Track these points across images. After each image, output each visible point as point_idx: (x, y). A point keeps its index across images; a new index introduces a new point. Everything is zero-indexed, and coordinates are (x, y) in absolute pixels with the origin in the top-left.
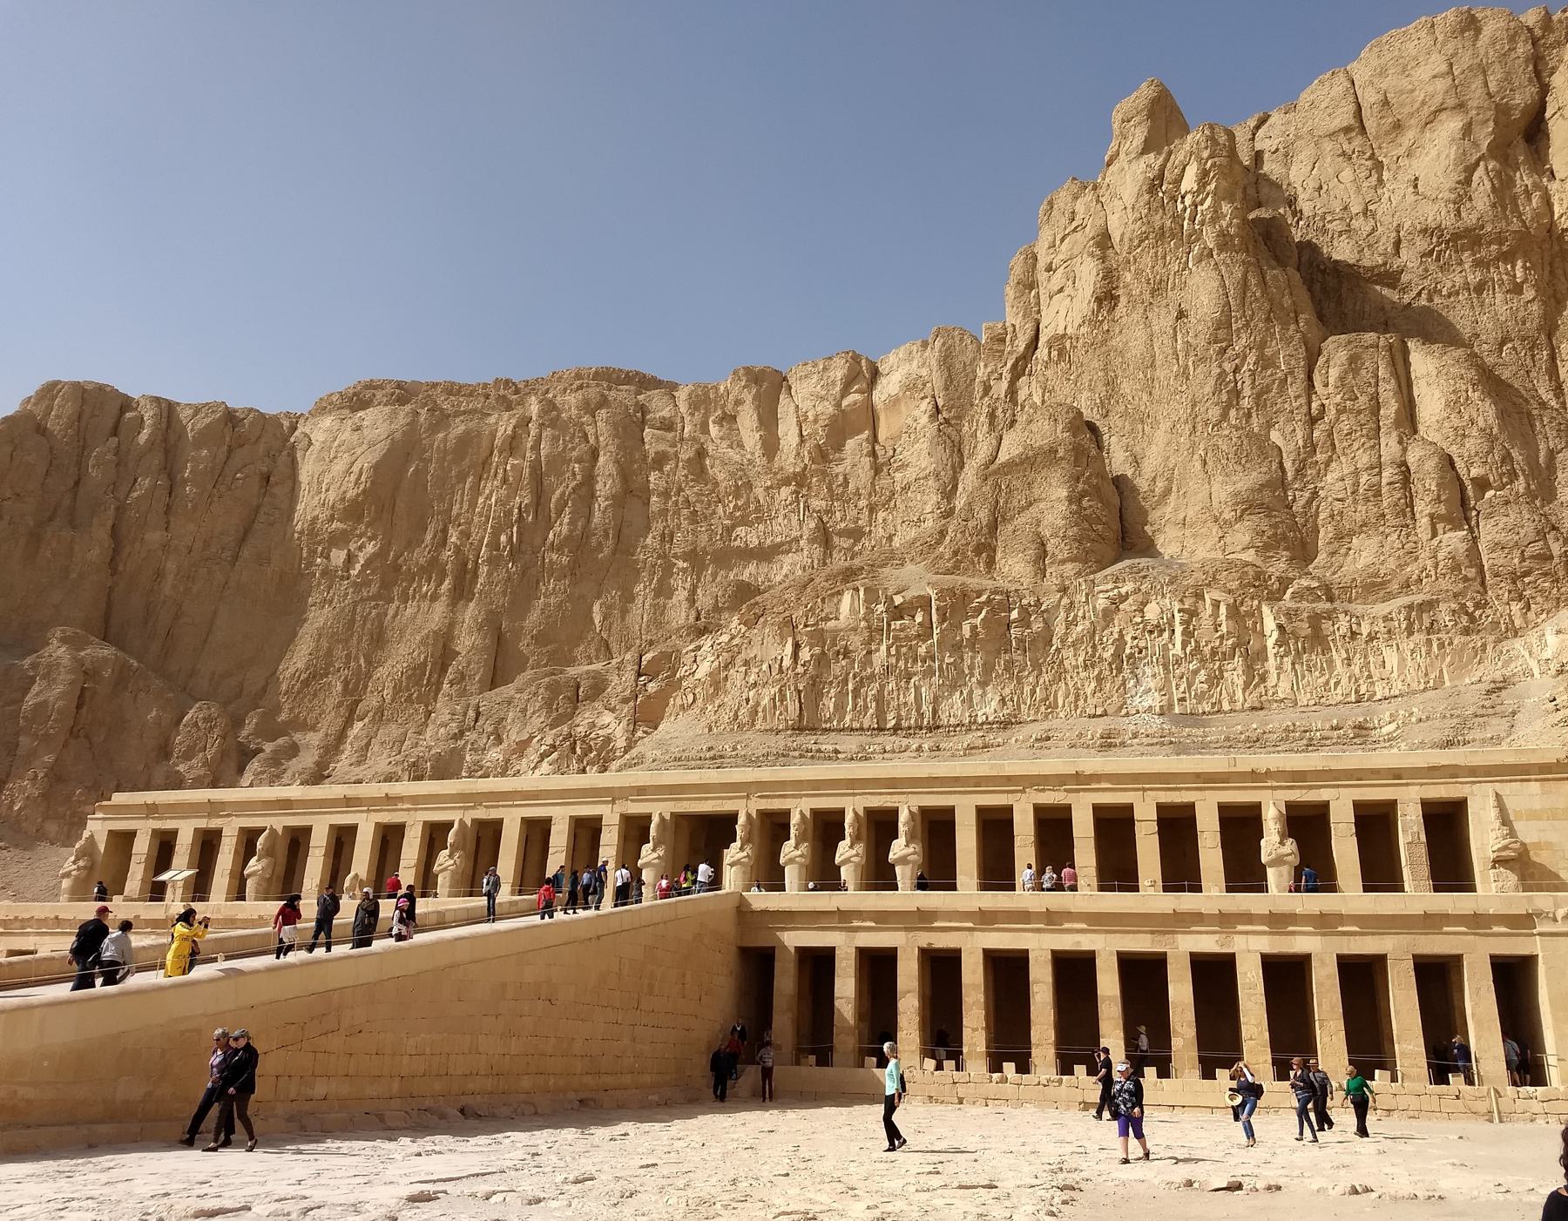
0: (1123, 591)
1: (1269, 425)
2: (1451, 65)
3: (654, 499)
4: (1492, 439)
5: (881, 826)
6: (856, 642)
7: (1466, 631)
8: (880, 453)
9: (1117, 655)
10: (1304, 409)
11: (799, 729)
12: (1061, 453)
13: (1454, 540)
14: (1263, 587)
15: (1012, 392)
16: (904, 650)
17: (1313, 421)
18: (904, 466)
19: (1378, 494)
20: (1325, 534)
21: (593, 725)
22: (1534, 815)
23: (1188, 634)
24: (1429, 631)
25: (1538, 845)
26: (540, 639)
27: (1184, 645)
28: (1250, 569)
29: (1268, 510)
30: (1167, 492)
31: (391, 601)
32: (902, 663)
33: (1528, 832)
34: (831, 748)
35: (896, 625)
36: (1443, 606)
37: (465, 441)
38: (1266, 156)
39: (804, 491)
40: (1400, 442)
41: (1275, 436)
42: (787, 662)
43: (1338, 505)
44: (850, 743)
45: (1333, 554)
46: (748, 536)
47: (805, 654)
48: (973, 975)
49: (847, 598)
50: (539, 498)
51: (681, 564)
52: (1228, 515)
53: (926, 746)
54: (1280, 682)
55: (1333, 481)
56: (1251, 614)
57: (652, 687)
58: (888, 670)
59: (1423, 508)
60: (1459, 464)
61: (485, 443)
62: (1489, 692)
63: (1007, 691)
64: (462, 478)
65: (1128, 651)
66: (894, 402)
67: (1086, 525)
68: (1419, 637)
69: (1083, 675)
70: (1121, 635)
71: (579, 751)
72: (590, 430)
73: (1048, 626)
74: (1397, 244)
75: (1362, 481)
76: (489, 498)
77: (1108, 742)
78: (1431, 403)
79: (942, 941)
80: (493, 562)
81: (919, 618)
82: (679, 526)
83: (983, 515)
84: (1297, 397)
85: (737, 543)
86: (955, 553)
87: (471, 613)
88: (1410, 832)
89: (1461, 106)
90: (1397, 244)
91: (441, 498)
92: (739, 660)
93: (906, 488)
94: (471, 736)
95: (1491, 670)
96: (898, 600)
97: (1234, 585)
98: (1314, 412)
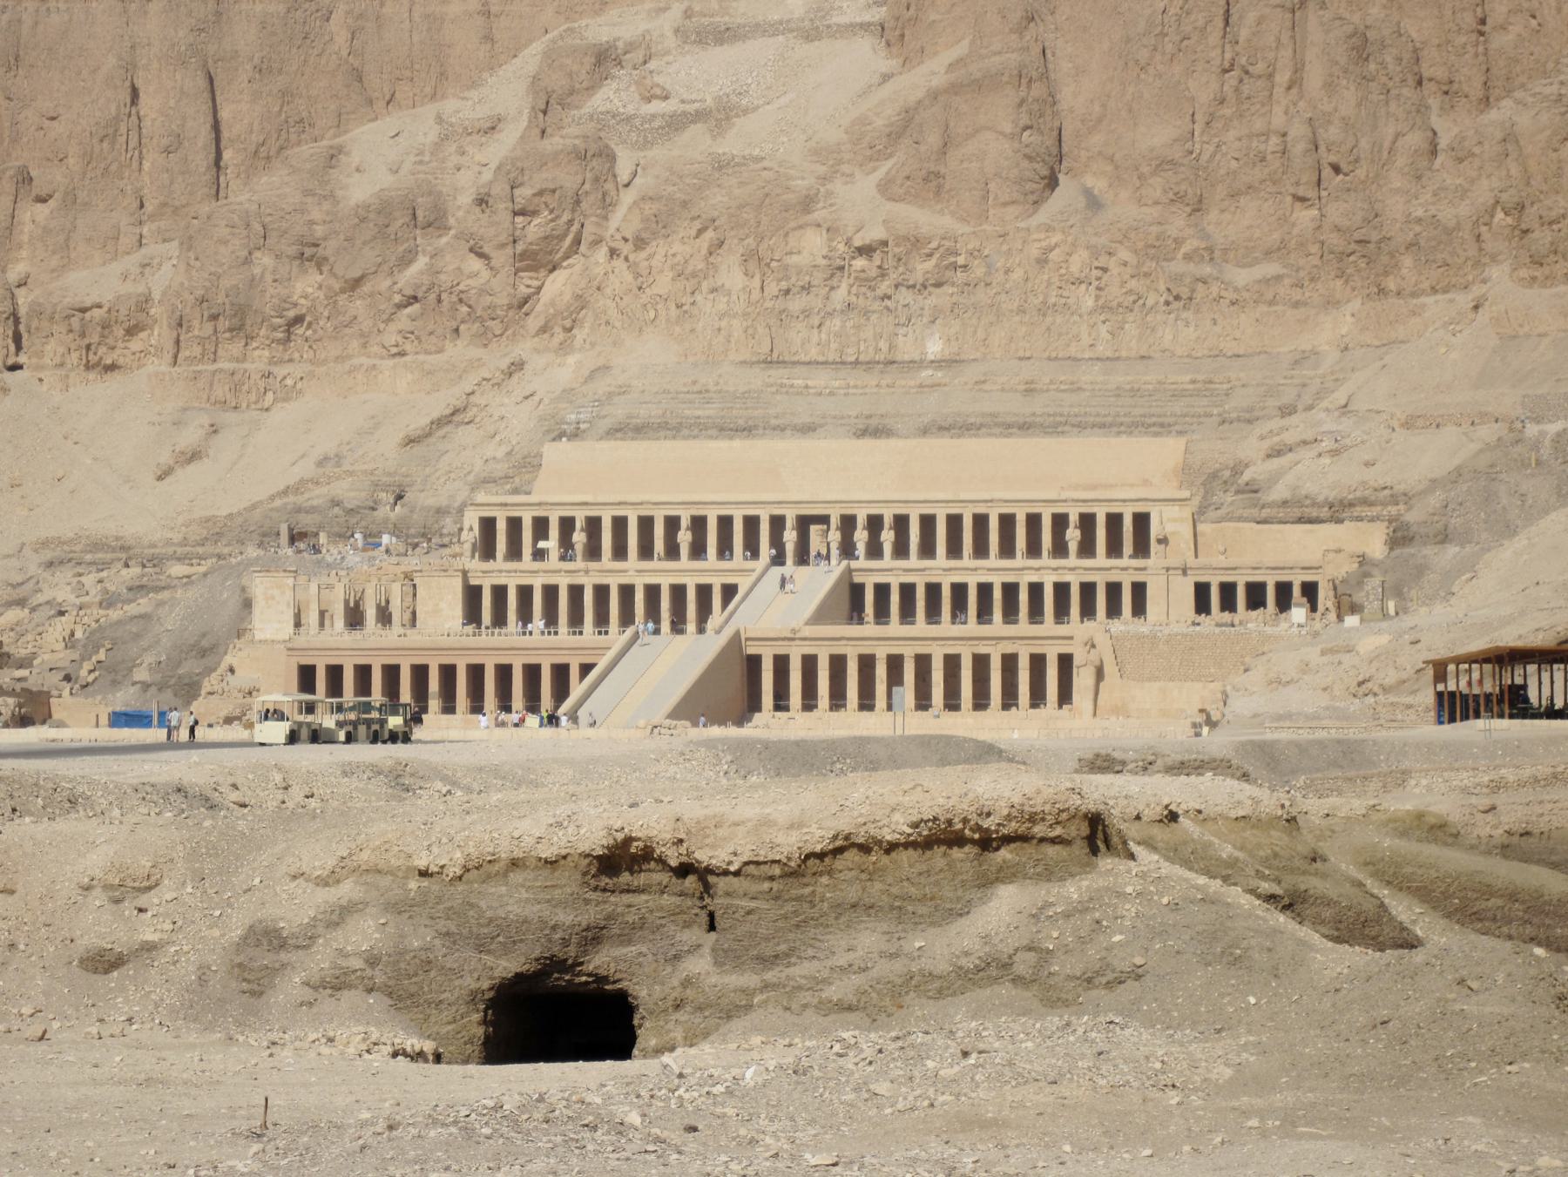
0: (1054, 241)
5: (901, 522)
7: (1296, 305)
9: (1044, 303)
10: (1218, 62)
11: (768, 363)
12: (1005, 79)
13: (1305, 217)
16: (863, 289)
17: (1226, 71)
19: (1263, 159)
20: (1221, 191)
22: (1175, 520)
23: (1099, 288)
24: (1271, 303)
25: (1173, 533)
27: (1097, 298)
28: (1155, 229)
30: (1100, 120)
32: (861, 301)
33: (1169, 528)
34: (800, 382)
35: (860, 263)
36: (1287, 281)
40: (1286, 113)
41: (1191, 83)
42: (756, 295)
43: (1234, 164)
44: (820, 379)
45: (1223, 211)
48: (946, 593)
53: (884, 383)
56: (1147, 275)
57: (534, 229)
60: (1322, 149)
62: (1296, 362)
63: (953, 331)
65: (1053, 300)
67: (1025, 164)
68: (1264, 308)
69: (1017, 318)
70: (1049, 284)
75: (1255, 144)
77: (1030, 390)
78: (1314, 78)
79: (934, 580)
81: (877, 257)
83: (933, 139)
84: (1214, 47)
86: (908, 178)
92: (705, 285)
94: (264, 260)
96: (858, 243)
97: (1140, 245)
98: (1227, 65)
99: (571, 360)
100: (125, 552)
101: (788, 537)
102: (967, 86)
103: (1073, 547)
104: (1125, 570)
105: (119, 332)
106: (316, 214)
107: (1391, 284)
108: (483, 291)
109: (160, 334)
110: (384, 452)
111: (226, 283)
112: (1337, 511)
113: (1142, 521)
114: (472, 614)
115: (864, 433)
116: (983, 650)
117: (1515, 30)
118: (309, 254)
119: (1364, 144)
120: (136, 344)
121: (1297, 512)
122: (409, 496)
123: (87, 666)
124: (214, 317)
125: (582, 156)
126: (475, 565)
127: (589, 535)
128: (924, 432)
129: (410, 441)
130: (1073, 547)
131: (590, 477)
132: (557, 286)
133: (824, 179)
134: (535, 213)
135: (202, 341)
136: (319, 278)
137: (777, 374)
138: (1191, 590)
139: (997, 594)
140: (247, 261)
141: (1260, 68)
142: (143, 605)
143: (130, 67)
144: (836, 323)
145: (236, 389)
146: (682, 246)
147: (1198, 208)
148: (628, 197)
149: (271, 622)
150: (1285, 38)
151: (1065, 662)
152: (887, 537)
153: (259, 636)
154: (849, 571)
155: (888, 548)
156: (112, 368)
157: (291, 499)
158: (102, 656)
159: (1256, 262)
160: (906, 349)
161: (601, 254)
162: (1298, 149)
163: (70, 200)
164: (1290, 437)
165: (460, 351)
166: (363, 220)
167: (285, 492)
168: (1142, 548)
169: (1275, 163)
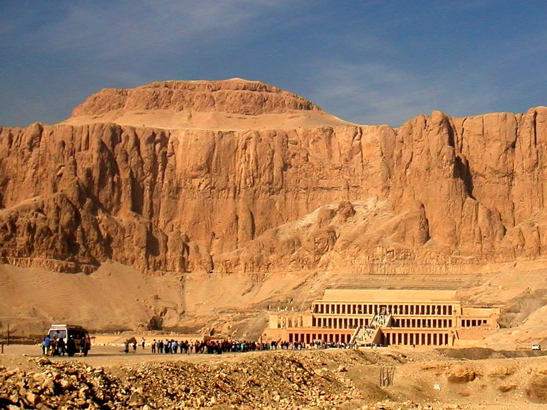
1: (455, 217)
2: (500, 129)
3: (293, 168)
4: (487, 229)
6: (380, 257)
8: (364, 161)
14: (450, 253)
15: (405, 173)
18: (371, 167)
20: (461, 241)
21: (303, 255)
26: (262, 213)
29: (452, 236)
31: (213, 198)
33: (456, 309)
35: (388, 254)
37: (230, 144)
38: (465, 131)
39: (341, 171)
46: (323, 183)
47: (370, 259)
48: (411, 321)
49: (378, 248)
50: (257, 167)
51: (303, 190)
52: (446, 236)
54: (451, 270)
55: (464, 231)
57: (319, 247)
58: (386, 263)
59: (475, 240)
61: (236, 144)
64: (230, 157)
66: (369, 146)
71: (301, 261)
72: (272, 144)
73: (414, 257)
74: (486, 168)
76: (240, 165)
78: (480, 219)
80: (246, 188)
82: (301, 178)
83: (403, 230)
85: (320, 186)
87: (241, 204)
88: (447, 308)
89: (500, 140)
90: (486, 168)
91: (224, 165)
92: (357, 258)
93: (372, 175)
94: (263, 252)
95: (478, 272)
96: (388, 250)
99: (327, 273)
100: (236, 310)
101: (381, 309)
102: (406, 221)
103: (436, 312)
104: (447, 317)
105: (233, 265)
106: (274, 243)
107: (497, 260)
108: (308, 259)
109: (242, 266)
110: (288, 291)
111: (255, 256)
112: (489, 306)
113: (450, 307)
114: (314, 324)
115: (389, 289)
116: (429, 333)
117: (520, 210)
118: (272, 251)
119: (490, 232)
120: (236, 268)
121: (481, 306)
122: (294, 300)
123: (233, 333)
124: (253, 263)
125: (329, 232)
126: (314, 314)
127: (338, 309)
128: (402, 289)
129: (294, 289)
130: (436, 312)
131: (333, 297)
132: (324, 258)
133: (381, 237)
134: (319, 243)
135: (251, 268)
136: (274, 255)
137: (373, 277)
138: (461, 321)
139: (421, 322)
140: (260, 251)
141: (469, 217)
142: (243, 321)
143: (235, 212)
144: (383, 267)
145: (257, 278)
146: (353, 249)
147: (457, 244)
148: (338, 240)
149: (273, 325)
150: (474, 211)
151: (446, 335)
152: (398, 310)
153: (271, 328)
154: (392, 317)
155: (398, 312)
156: (231, 273)
157: (270, 300)
158: (236, 331)
159: (469, 255)
160: (398, 271)
161: (333, 252)
162: (477, 232)
163: (223, 239)
164: (479, 291)
165: (303, 271)
166: (284, 244)
167: (269, 299)
168: (450, 313)
169: (472, 236)
